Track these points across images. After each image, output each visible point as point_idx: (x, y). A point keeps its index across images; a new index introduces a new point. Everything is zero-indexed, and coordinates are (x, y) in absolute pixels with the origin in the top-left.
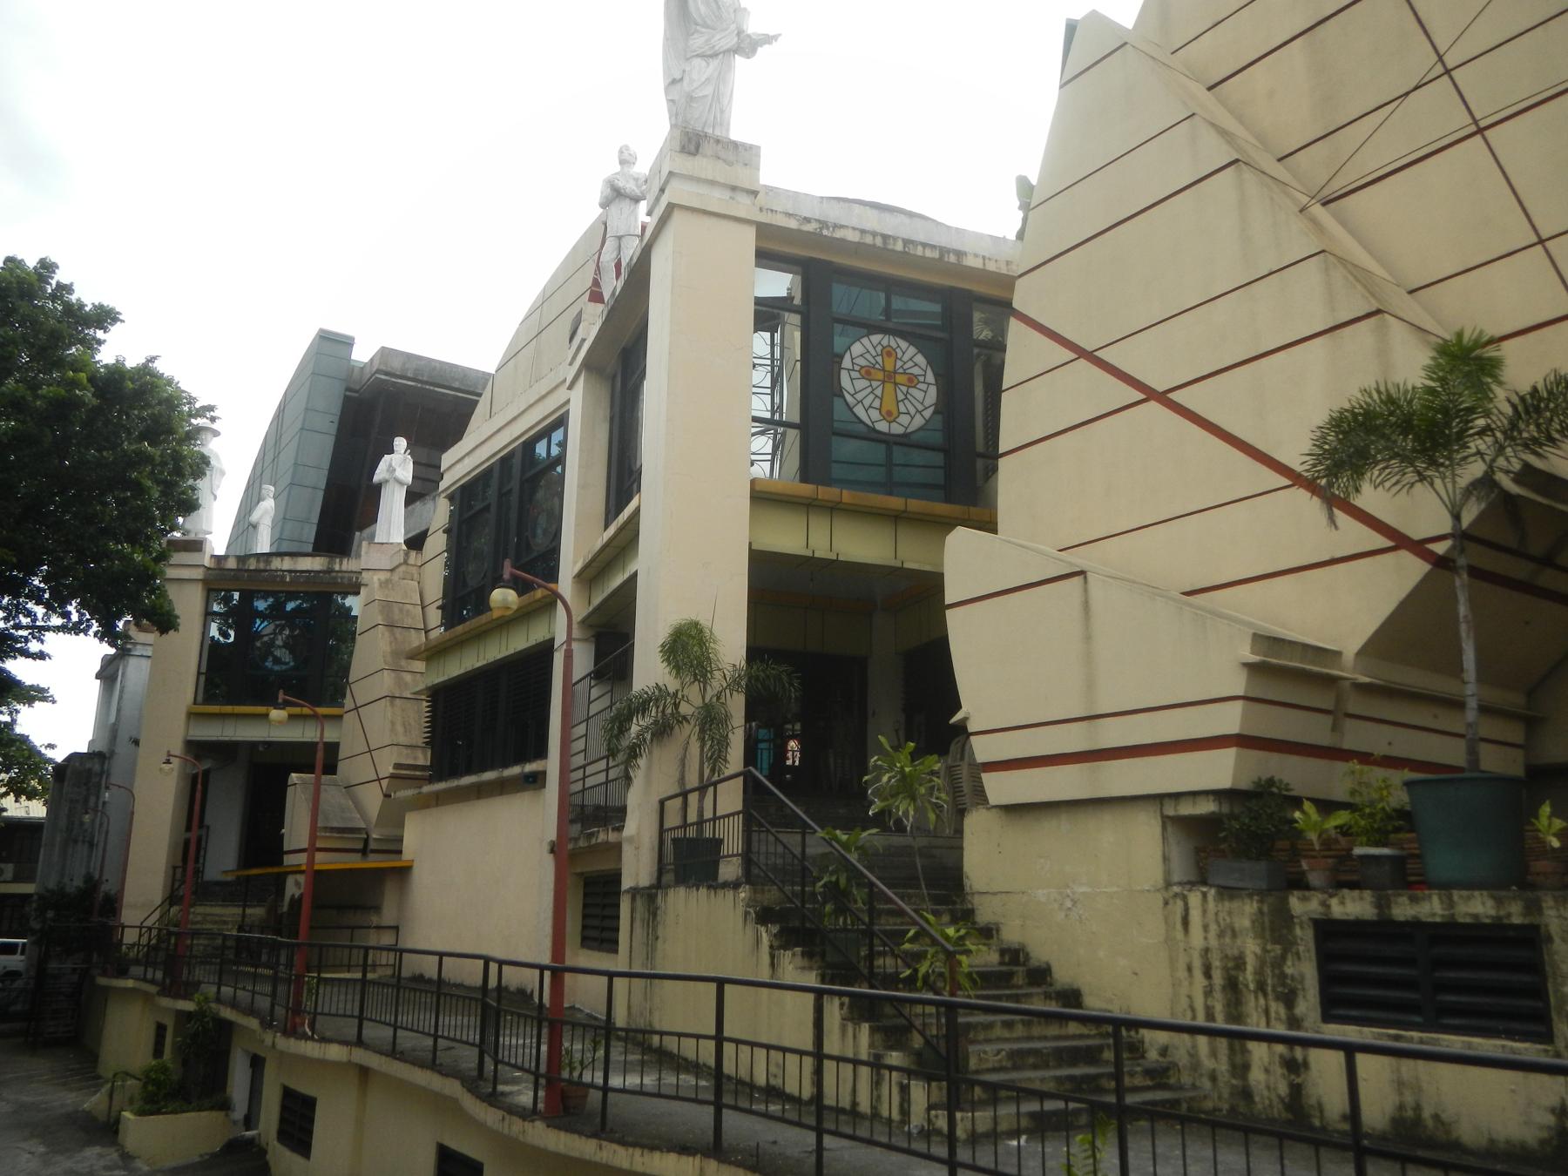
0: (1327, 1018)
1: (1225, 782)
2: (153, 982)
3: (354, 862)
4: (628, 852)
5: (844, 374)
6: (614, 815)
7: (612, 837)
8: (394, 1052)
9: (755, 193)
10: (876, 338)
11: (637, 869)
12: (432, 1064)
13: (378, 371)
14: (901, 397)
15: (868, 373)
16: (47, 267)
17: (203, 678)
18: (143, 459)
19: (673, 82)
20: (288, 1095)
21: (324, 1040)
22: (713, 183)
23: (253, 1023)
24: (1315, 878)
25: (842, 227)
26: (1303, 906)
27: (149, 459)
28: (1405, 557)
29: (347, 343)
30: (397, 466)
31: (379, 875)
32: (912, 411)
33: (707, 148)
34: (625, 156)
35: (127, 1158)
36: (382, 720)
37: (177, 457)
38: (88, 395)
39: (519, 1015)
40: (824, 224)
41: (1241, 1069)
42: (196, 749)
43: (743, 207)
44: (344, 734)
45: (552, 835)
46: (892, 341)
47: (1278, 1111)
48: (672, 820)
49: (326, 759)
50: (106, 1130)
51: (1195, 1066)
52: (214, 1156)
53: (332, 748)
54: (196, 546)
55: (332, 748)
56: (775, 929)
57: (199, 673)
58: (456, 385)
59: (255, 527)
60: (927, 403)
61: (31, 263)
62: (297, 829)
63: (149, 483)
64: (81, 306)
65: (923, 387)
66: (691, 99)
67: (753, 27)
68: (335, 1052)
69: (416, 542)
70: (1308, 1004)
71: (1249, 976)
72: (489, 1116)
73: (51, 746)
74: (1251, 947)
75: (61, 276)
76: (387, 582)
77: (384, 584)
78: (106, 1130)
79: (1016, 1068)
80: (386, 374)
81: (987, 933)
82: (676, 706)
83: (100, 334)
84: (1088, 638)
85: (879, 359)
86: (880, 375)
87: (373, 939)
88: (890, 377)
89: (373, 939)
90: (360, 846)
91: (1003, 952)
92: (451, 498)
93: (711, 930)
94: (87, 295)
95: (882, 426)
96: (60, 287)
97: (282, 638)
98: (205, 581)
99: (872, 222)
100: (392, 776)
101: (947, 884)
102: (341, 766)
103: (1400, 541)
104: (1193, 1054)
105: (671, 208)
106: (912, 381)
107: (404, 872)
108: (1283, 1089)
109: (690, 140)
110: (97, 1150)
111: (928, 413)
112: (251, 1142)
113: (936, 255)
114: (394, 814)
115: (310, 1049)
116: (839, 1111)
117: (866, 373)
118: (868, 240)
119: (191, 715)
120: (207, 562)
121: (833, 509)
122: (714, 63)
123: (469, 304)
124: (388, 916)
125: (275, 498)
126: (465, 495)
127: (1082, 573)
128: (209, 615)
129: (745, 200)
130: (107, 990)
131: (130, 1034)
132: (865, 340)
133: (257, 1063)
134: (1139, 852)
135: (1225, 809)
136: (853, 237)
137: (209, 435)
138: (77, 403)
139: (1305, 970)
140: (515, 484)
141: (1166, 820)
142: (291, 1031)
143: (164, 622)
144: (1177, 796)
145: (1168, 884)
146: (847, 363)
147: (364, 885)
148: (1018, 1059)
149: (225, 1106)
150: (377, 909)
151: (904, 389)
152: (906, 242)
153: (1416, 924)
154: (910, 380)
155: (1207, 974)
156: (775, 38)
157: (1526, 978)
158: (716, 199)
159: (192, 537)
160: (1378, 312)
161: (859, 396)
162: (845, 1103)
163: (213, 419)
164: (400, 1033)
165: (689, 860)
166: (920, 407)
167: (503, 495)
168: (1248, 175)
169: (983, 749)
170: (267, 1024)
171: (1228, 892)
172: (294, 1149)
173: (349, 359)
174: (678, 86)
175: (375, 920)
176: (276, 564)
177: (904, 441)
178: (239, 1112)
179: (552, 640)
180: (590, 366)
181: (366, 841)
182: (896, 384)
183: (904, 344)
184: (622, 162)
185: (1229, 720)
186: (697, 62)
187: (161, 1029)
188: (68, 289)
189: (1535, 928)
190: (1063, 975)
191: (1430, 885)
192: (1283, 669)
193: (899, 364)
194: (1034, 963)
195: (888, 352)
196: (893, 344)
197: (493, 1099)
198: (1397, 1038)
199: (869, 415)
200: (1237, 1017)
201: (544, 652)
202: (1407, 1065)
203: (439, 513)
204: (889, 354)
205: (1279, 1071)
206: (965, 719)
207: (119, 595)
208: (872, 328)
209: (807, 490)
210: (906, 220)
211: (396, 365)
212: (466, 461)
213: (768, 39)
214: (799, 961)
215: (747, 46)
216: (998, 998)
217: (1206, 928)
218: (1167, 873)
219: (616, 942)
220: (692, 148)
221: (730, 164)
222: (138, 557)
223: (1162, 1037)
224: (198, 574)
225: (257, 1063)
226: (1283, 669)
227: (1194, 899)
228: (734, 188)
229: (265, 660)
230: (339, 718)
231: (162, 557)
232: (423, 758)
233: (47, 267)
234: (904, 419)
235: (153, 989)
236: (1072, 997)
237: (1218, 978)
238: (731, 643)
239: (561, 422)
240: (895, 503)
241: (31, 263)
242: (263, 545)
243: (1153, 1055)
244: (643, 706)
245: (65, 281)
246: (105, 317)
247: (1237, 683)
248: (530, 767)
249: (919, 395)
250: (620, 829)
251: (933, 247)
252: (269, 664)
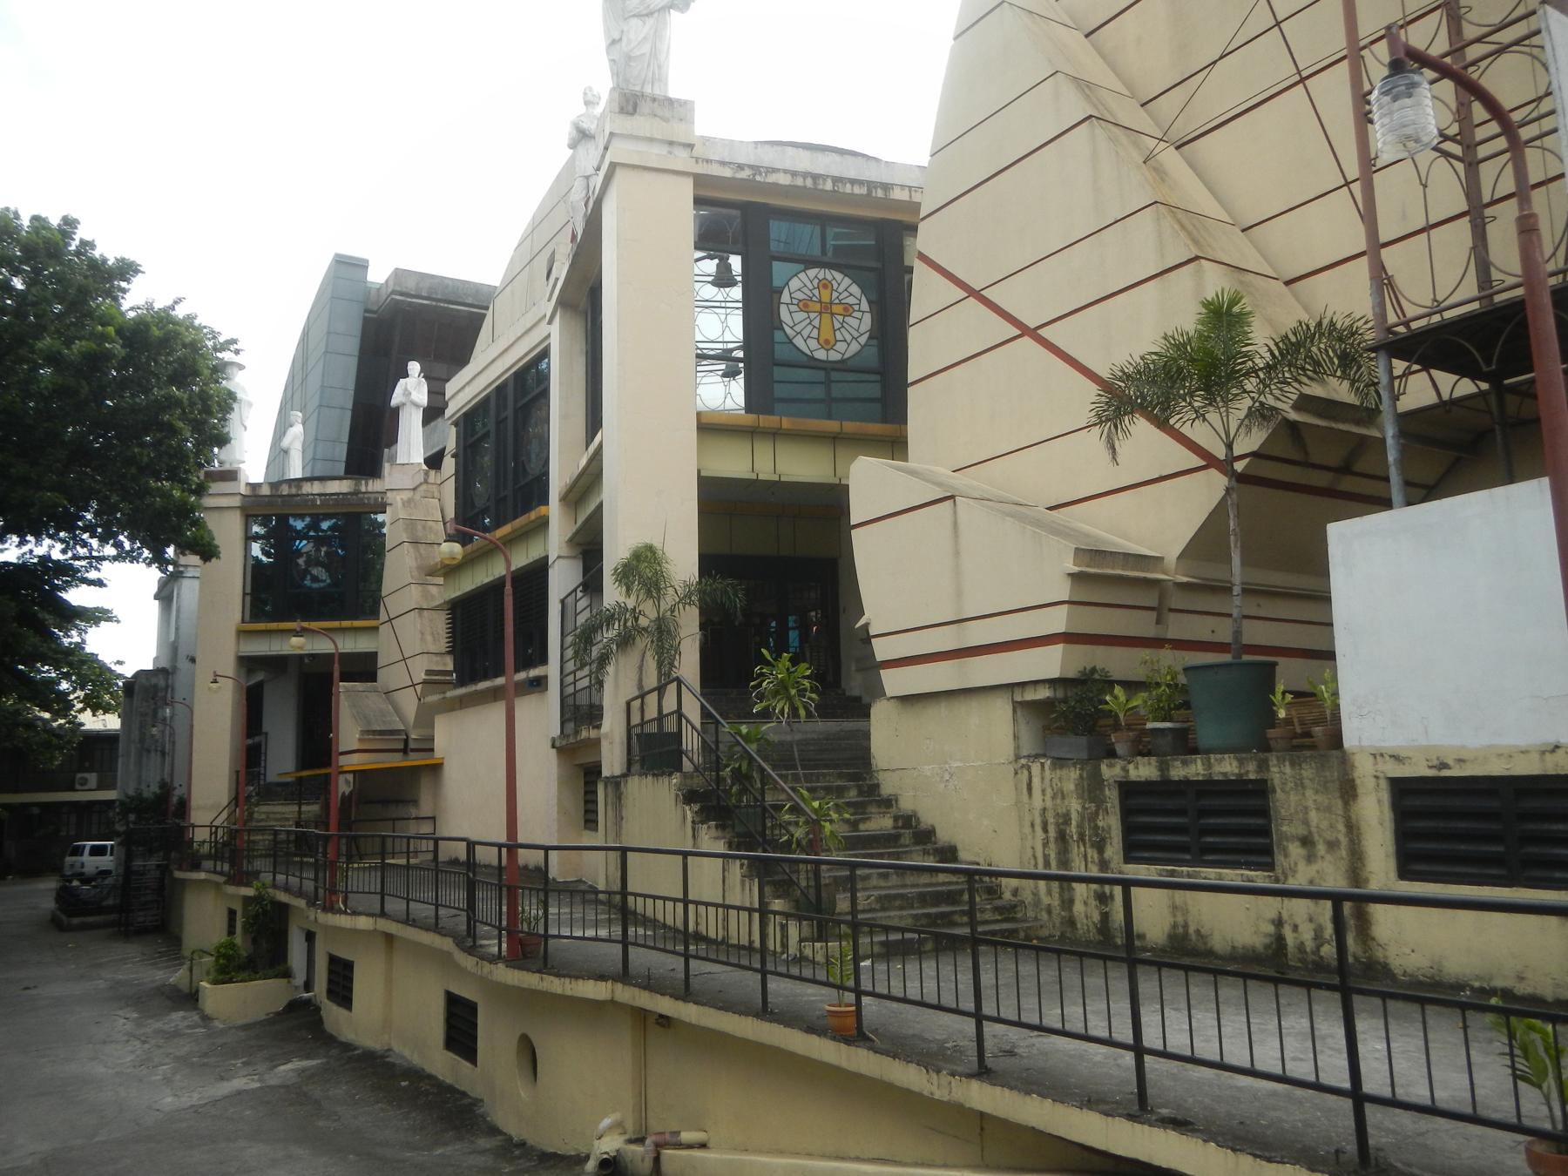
0: (1128, 859)
1: (1055, 673)
2: (221, 873)
3: (396, 761)
4: (605, 745)
5: (783, 309)
6: (593, 715)
7: (593, 734)
8: (408, 920)
9: (691, 146)
10: (812, 272)
11: (612, 760)
12: (436, 927)
13: (393, 292)
14: (837, 325)
15: (806, 306)
16: (69, 224)
17: (248, 598)
18: (171, 403)
20: (333, 960)
21: (355, 913)
22: (651, 140)
23: (301, 903)
24: (1120, 749)
25: (775, 170)
26: (1110, 771)
27: (178, 403)
28: (1213, 473)
29: (361, 265)
30: (412, 389)
31: (415, 771)
32: (849, 338)
33: (645, 107)
34: (590, 97)
35: (206, 1019)
36: (410, 631)
37: (204, 397)
38: (117, 348)
39: (531, 889)
40: (756, 169)
41: (1068, 903)
42: (248, 663)
43: (681, 160)
44: (381, 644)
45: (556, 732)
46: (828, 274)
47: (1093, 935)
48: (636, 720)
49: (363, 668)
50: (189, 999)
51: (1037, 903)
52: (278, 1014)
53: (373, 656)
54: (231, 475)
55: (373, 656)
56: (696, 807)
57: (245, 594)
58: (470, 301)
59: (286, 452)
60: (862, 330)
61: (55, 221)
62: (348, 733)
63: (181, 424)
64: (105, 261)
65: (858, 315)
66: (629, 58)
68: (363, 923)
69: (434, 461)
70: (1114, 850)
71: (1073, 829)
72: (468, 962)
73: (120, 663)
74: (1075, 806)
75: (81, 234)
76: (410, 501)
77: (407, 503)
78: (189, 999)
79: (883, 909)
80: (402, 294)
81: (888, 803)
82: (637, 619)
83: (124, 284)
84: (957, 553)
85: (816, 292)
86: (818, 307)
87: (413, 829)
88: (826, 308)
89: (413, 829)
90: (401, 746)
91: (896, 819)
92: (456, 424)
93: (655, 810)
94: (108, 250)
95: (821, 355)
96: (84, 243)
97: (316, 562)
98: (242, 508)
99: (805, 162)
100: (425, 682)
101: (851, 764)
102: (380, 673)
103: (1210, 461)
104: (1035, 894)
105: (613, 166)
106: (848, 310)
107: (436, 769)
108: (1096, 917)
109: (627, 101)
110: (182, 1013)
111: (863, 340)
112: (308, 1002)
113: (864, 191)
114: (426, 716)
115: (343, 921)
116: (739, 947)
117: (804, 306)
118: (799, 182)
119: (241, 633)
120: (243, 490)
121: (775, 435)
122: (650, 21)
123: (470, 234)
124: (425, 809)
125: (304, 424)
126: (468, 422)
127: (952, 497)
128: (249, 538)
129: (682, 154)
130: (183, 881)
131: (207, 917)
132: (802, 275)
133: (310, 937)
134: (996, 729)
135: (1060, 694)
136: (784, 180)
137: (235, 369)
138: (107, 356)
139: (1112, 822)
140: (510, 412)
141: (1017, 705)
142: (330, 908)
143: (207, 552)
144: (1023, 685)
145: (1018, 757)
146: (785, 297)
147: (404, 781)
148: (886, 902)
149: (287, 974)
150: (415, 802)
151: (840, 318)
152: (837, 180)
153: (1186, 783)
154: (846, 309)
155: (1045, 830)
157: (1260, 821)
158: (655, 155)
159: (227, 467)
160: (1197, 258)
161: (798, 328)
162: (744, 941)
163: (237, 352)
164: (412, 904)
165: (654, 750)
166: (856, 334)
167: (500, 422)
168: (1099, 130)
169: (883, 650)
170: (312, 903)
171: (1059, 763)
172: (339, 1005)
173: (365, 281)
174: (618, 46)
175: (414, 812)
176: (307, 488)
177: (842, 366)
178: (300, 979)
179: (547, 557)
180: (564, 303)
181: (406, 741)
182: (832, 314)
183: (839, 276)
184: (587, 103)
185: (1057, 621)
186: (635, 22)
187: (232, 914)
188: (91, 245)
189: (1264, 782)
190: (943, 836)
191: (1195, 751)
192: (1104, 576)
193: (835, 295)
194: (923, 826)
195: (825, 284)
196: (829, 277)
197: (472, 950)
198: (1172, 874)
199: (808, 345)
200: (1064, 862)
201: (539, 570)
202: (1179, 895)
203: (450, 439)
204: (825, 287)
205: (1093, 902)
206: (866, 626)
207: (166, 529)
208: (809, 263)
209: (751, 419)
210: (837, 157)
211: (410, 285)
212: (467, 389)
214: (713, 832)
216: (881, 856)
217: (1043, 791)
218: (1017, 748)
219: (596, 822)
220: (630, 108)
221: (666, 120)
222: (177, 493)
223: (1014, 882)
224: (236, 502)
225: (310, 937)
226: (1104, 576)
227: (1036, 768)
228: (671, 143)
229: (303, 579)
230: (376, 629)
231: (200, 490)
232: (449, 664)
233: (69, 224)
234: (841, 347)
235: (221, 879)
236: (949, 853)
237: (1052, 833)
238: (683, 563)
239: (545, 354)
240: (832, 426)
241: (55, 221)
242: (296, 470)
243: (1007, 896)
244: (610, 619)
245: (88, 238)
246: (127, 270)
247: (1063, 591)
248: (534, 673)
249: (854, 323)
250: (599, 727)
251: (861, 183)
252: (307, 583)
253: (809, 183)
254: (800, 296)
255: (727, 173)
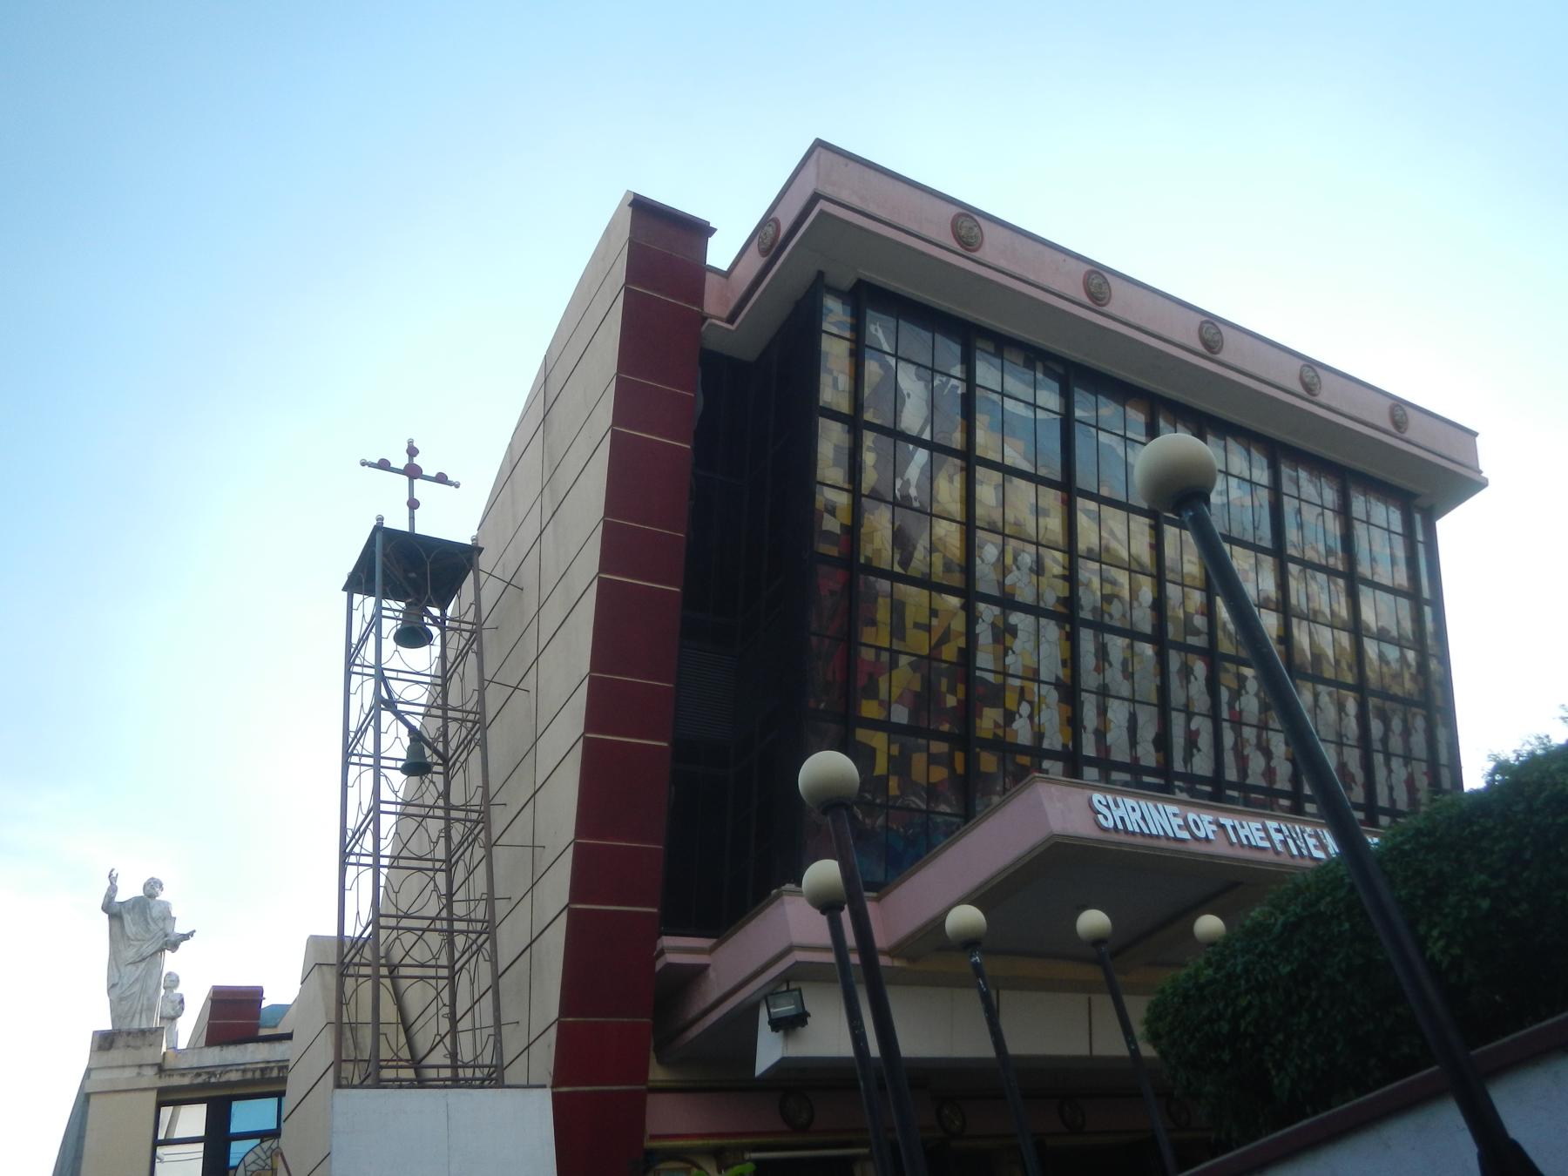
10: (266, 1145)
19: (112, 987)
33: (120, 1042)
67: (180, 928)
118: (249, 1075)
136: (234, 1076)
156: (192, 934)
213: (186, 937)
215: (174, 946)
221: (137, 1048)
228: (140, 1066)
253: (258, 1075)
254: (254, 1167)
255: (186, 1081)
